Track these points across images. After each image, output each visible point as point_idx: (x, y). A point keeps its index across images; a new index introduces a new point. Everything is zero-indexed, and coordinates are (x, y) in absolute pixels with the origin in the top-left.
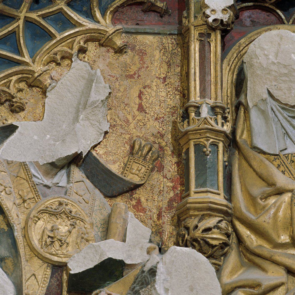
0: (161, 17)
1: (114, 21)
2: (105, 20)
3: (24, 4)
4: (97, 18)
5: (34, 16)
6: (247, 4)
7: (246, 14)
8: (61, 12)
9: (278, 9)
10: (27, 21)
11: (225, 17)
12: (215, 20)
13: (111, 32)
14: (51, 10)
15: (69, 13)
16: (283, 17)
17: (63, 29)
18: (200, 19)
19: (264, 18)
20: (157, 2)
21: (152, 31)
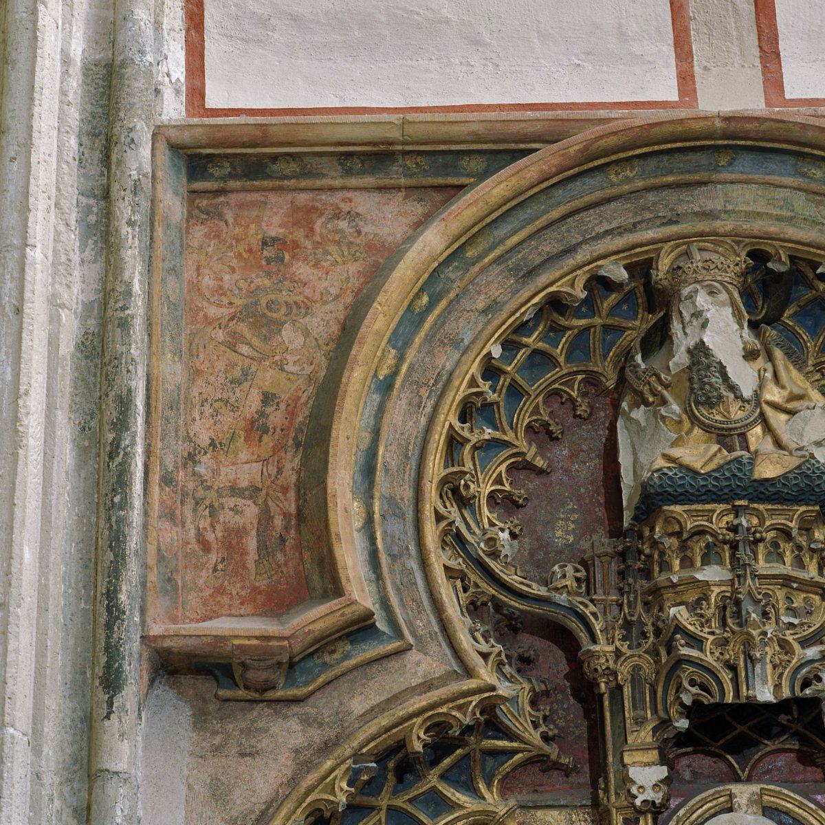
0: (567, 777)
1: (505, 791)
2: (492, 793)
3: (385, 788)
4: (481, 793)
5: (399, 802)
6: (683, 750)
7: (684, 761)
8: (434, 790)
9: (729, 754)
10: (390, 808)
11: (658, 797)
12: (644, 801)
13: (502, 813)
14: (421, 791)
15: (445, 792)
16: (736, 766)
17: (435, 815)
18: (623, 799)
19: (710, 766)
20: (560, 758)
21: (556, 803)
